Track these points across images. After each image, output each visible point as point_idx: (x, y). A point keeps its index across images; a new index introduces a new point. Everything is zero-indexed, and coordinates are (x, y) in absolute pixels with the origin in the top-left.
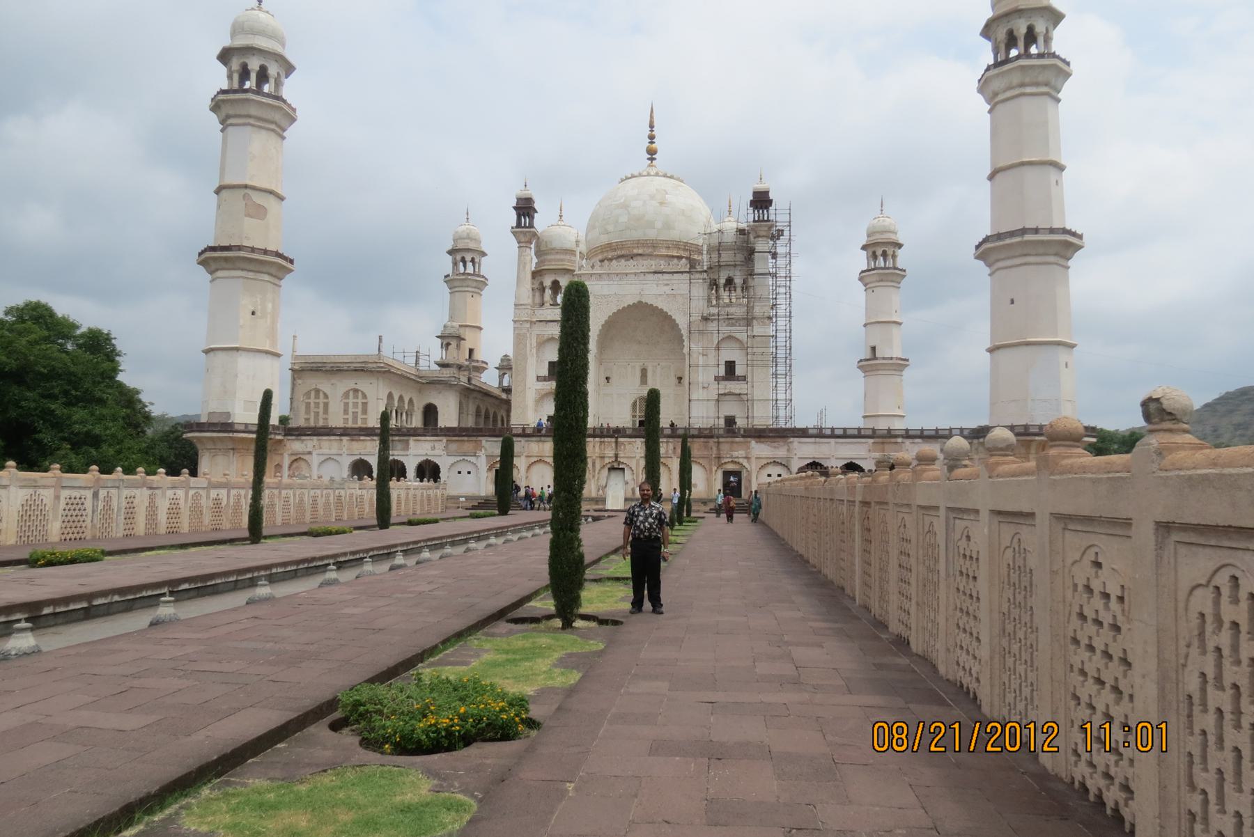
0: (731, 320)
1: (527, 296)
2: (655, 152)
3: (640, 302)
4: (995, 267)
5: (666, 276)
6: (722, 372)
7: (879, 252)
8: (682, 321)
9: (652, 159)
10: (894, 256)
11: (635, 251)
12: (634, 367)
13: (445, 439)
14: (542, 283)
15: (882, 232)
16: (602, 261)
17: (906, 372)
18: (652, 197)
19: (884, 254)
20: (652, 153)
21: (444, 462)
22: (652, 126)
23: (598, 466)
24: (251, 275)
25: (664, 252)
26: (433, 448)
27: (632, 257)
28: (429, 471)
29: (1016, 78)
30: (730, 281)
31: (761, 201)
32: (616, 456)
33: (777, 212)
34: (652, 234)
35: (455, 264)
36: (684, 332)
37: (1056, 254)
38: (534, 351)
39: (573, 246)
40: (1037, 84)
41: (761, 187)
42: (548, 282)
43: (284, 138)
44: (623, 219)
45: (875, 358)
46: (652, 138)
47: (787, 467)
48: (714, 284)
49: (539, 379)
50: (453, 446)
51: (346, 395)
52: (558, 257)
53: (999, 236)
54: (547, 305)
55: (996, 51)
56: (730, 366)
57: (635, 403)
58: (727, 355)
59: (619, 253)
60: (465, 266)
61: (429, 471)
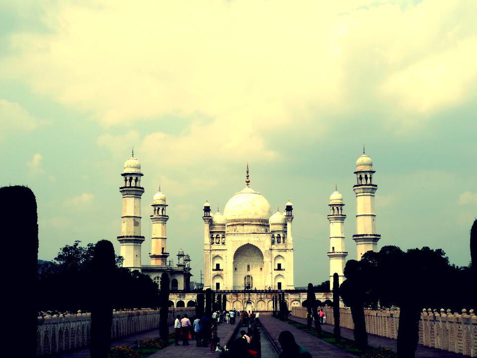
0: (280, 250)
2: (249, 182)
6: (276, 268)
7: (335, 208)
8: (263, 250)
10: (341, 209)
11: (245, 223)
14: (213, 235)
19: (337, 208)
22: (248, 172)
23: (244, 302)
24: (136, 244)
25: (254, 223)
26: (193, 297)
29: (362, 191)
32: (249, 298)
34: (250, 217)
35: (155, 210)
36: (263, 254)
37: (373, 241)
38: (211, 260)
40: (367, 192)
41: (289, 204)
42: (215, 236)
43: (141, 198)
47: (299, 301)
48: (273, 237)
49: (213, 270)
51: (155, 279)
52: (218, 226)
53: (358, 236)
54: (215, 244)
56: (279, 265)
57: (245, 278)
58: (279, 261)
59: (239, 223)
60: (158, 210)
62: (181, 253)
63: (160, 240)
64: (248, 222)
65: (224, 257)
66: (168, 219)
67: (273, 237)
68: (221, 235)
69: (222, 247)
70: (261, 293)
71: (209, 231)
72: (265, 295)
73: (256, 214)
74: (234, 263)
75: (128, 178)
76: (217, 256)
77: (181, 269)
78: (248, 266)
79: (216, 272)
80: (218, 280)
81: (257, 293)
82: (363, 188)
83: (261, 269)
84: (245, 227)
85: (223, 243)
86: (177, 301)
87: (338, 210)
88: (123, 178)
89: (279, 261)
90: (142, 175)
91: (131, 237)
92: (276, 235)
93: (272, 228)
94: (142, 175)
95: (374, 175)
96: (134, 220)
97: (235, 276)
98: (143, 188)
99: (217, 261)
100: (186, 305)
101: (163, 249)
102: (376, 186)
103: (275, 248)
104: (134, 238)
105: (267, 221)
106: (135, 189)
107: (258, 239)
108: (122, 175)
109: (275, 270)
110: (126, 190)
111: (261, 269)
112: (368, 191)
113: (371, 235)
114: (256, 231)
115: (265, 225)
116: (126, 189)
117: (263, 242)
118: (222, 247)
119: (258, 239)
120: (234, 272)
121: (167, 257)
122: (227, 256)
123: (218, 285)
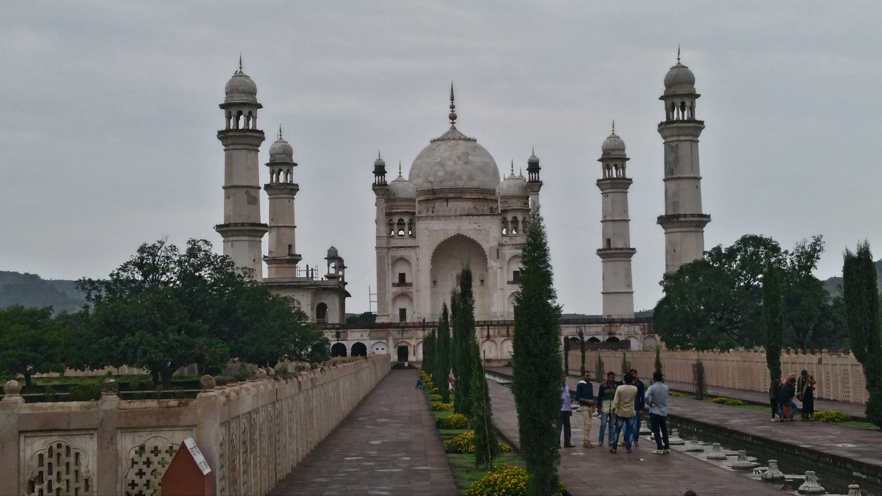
1: (384, 230)
3: (459, 234)
4: (669, 230)
5: (475, 218)
8: (486, 247)
9: (453, 123)
10: (624, 168)
11: (450, 195)
12: (452, 274)
13: (368, 330)
15: (613, 150)
16: (427, 200)
17: (634, 259)
18: (459, 158)
19: (616, 166)
20: (453, 117)
21: (368, 343)
22: (452, 99)
24: (252, 239)
26: (362, 336)
27: (447, 200)
28: (360, 349)
29: (675, 132)
30: (515, 218)
31: (534, 167)
33: (543, 176)
34: (460, 184)
36: (487, 253)
39: (414, 196)
40: (686, 135)
42: (396, 220)
44: (441, 174)
45: (611, 249)
46: (453, 107)
48: (505, 223)
49: (394, 285)
50: (374, 335)
55: (666, 109)
59: (438, 196)
60: (278, 174)
61: (360, 349)
62: (332, 255)
63: (283, 230)
64: (459, 194)
65: (413, 260)
66: (298, 190)
67: (505, 218)
68: (406, 220)
69: (410, 242)
70: (488, 326)
71: (384, 212)
72: (497, 331)
73: (471, 178)
74: (432, 271)
75: (234, 112)
76: (402, 259)
77: (333, 283)
79: (398, 290)
80: (402, 304)
81: (482, 326)
82: (678, 128)
83: (482, 281)
84: (452, 204)
85: (413, 236)
86: (333, 343)
87: (617, 169)
88: (223, 112)
90: (260, 106)
91: (243, 224)
92: (510, 218)
93: (500, 206)
94: (260, 106)
95: (698, 101)
96: (247, 193)
97: (433, 294)
98: (262, 132)
99: (401, 268)
100: (349, 352)
101: (291, 247)
102: (702, 123)
103: (509, 242)
104: (249, 228)
105: (492, 192)
106: (247, 134)
107: (476, 226)
108: (222, 106)
109: (509, 283)
110: (231, 136)
111: (482, 281)
112: (688, 132)
113: (693, 215)
114: (472, 212)
115: (487, 200)
116: (231, 134)
118: (410, 242)
119: (476, 226)
120: (432, 287)
121: (297, 261)
122: (420, 258)
123: (403, 312)
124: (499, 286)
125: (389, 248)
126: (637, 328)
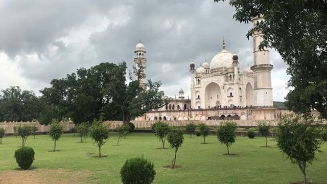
8: (220, 86)
21: (167, 117)
30: (231, 75)
34: (219, 67)
56: (231, 94)
58: (230, 91)
73: (222, 64)
76: (198, 91)
78: (218, 96)
79: (197, 100)
80: (198, 105)
89: (230, 91)
99: (198, 94)
109: (228, 97)
113: (260, 65)
117: (220, 80)
118: (199, 86)
123: (199, 107)
124: (224, 98)
125: (194, 88)
126: (245, 111)
